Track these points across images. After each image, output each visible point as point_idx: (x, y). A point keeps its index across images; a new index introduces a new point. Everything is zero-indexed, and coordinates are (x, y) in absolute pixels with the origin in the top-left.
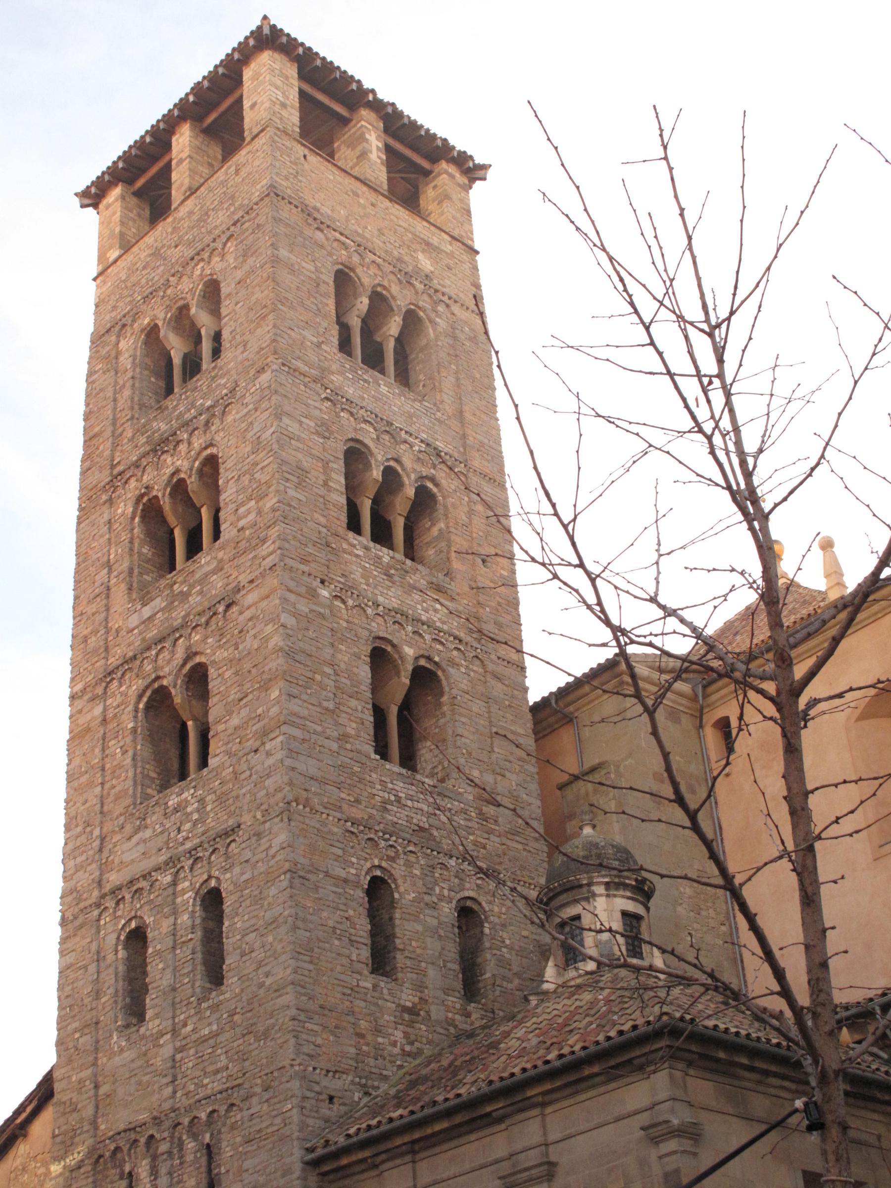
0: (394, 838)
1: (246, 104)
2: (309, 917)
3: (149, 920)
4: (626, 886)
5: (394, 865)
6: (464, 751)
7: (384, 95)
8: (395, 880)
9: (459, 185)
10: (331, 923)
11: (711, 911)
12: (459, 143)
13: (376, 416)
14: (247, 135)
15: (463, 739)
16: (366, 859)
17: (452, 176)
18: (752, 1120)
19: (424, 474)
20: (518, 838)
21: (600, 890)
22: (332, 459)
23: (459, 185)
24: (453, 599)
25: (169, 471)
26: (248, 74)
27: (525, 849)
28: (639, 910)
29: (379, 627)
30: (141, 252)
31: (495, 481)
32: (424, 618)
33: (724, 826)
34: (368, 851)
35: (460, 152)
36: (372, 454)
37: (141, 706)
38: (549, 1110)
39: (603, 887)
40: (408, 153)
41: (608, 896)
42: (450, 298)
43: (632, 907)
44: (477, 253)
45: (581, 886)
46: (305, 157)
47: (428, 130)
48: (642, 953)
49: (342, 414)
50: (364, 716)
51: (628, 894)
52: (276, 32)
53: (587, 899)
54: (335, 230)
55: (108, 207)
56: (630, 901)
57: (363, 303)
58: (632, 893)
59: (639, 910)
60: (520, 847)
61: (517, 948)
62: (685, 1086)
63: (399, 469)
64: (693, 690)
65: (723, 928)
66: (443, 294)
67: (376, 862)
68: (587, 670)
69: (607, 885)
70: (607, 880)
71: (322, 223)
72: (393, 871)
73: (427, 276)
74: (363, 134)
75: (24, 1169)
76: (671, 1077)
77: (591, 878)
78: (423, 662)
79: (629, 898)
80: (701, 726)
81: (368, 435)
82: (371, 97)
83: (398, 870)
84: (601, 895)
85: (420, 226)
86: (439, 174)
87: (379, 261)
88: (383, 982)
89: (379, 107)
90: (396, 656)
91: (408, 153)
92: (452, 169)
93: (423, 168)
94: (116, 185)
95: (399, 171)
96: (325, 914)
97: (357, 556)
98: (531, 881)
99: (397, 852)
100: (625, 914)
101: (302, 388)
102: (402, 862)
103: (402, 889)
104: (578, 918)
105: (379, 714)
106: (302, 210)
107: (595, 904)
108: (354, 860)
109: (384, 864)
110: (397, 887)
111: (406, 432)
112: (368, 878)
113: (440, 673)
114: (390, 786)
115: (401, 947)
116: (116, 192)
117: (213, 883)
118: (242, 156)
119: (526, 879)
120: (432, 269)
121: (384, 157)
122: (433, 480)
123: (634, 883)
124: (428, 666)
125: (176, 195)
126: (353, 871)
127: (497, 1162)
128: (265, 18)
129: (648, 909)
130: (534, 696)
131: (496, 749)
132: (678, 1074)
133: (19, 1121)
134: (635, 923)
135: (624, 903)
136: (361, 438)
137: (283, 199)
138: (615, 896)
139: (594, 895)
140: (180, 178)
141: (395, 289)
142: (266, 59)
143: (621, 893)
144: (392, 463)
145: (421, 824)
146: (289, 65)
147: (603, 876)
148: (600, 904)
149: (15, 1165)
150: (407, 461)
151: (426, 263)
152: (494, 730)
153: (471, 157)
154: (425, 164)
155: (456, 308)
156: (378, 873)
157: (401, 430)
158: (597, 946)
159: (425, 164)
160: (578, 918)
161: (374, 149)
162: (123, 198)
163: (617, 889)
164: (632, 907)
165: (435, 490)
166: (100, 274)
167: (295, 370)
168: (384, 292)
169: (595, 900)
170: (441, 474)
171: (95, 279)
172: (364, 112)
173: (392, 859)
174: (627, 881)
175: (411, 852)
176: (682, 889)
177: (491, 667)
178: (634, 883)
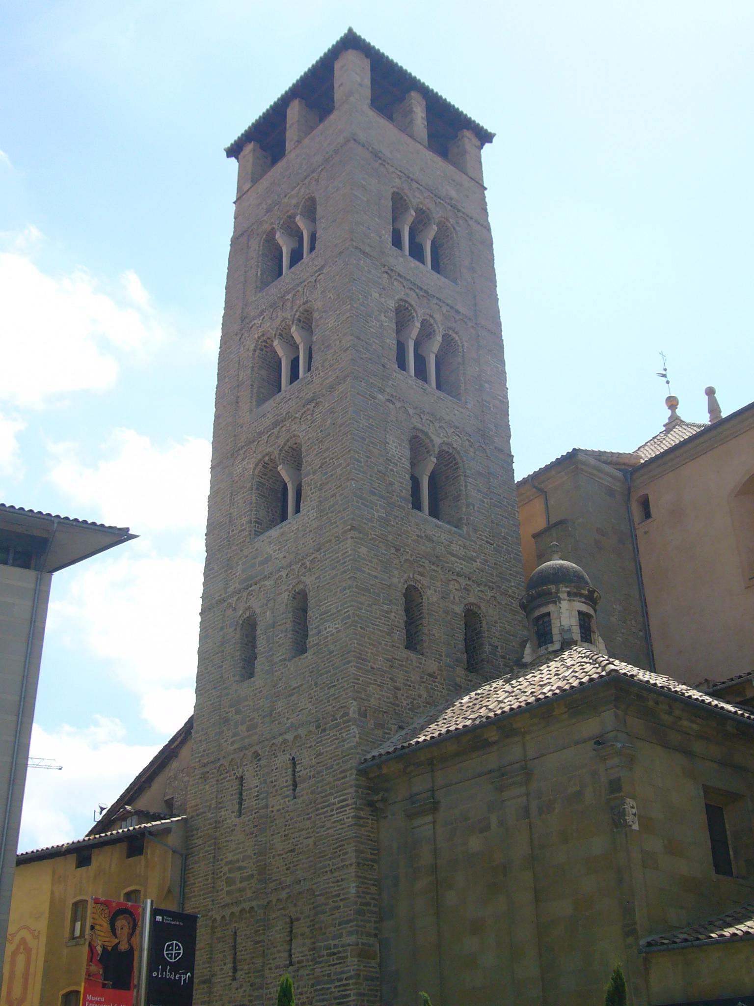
1: (336, 86)
3: (258, 610)
4: (581, 595)
9: (475, 146)
11: (633, 622)
14: (336, 105)
17: (470, 139)
18: (670, 748)
21: (563, 596)
23: (475, 146)
25: (278, 321)
26: (337, 66)
28: (591, 611)
29: (416, 422)
30: (264, 183)
33: (643, 566)
37: (256, 472)
38: (528, 737)
39: (566, 594)
41: (570, 600)
42: (467, 216)
43: (585, 608)
44: (486, 189)
45: (551, 593)
48: (591, 640)
49: (395, 283)
51: (583, 600)
53: (555, 602)
55: (244, 156)
57: (411, 215)
58: (586, 599)
59: (591, 611)
62: (625, 722)
63: (432, 321)
64: (624, 476)
65: (641, 634)
66: (464, 213)
68: (554, 460)
69: (569, 594)
70: (568, 589)
71: (384, 161)
74: (412, 108)
75: (175, 778)
76: (616, 715)
78: (445, 448)
79: (583, 602)
80: (629, 499)
81: (413, 300)
84: (565, 600)
85: (450, 168)
86: (463, 137)
87: (421, 187)
88: (413, 656)
94: (250, 142)
104: (548, 614)
105: (415, 483)
107: (560, 605)
115: (426, 632)
116: (250, 147)
117: (301, 586)
118: (333, 117)
121: (426, 123)
123: (587, 592)
125: (289, 146)
127: (490, 772)
129: (595, 611)
130: (518, 478)
132: (620, 713)
133: (173, 747)
134: (587, 619)
135: (580, 606)
138: (574, 601)
139: (560, 599)
140: (291, 134)
141: (432, 206)
142: (351, 57)
143: (578, 598)
144: (428, 318)
148: (564, 605)
149: (170, 775)
150: (438, 317)
151: (453, 194)
155: (471, 222)
156: (412, 583)
158: (561, 634)
160: (548, 614)
162: (254, 150)
164: (585, 608)
166: (238, 199)
169: (560, 603)
171: (235, 203)
172: (414, 94)
176: (615, 607)
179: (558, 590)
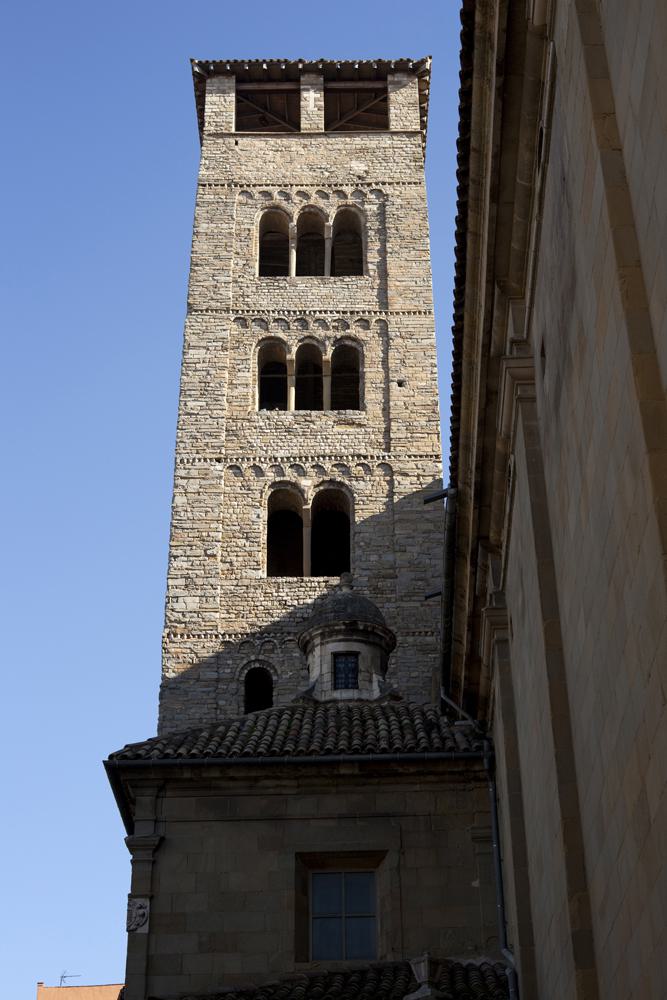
0: (272, 635)
2: (176, 716)
4: (338, 632)
5: (272, 655)
6: (362, 544)
7: (311, 58)
8: (273, 667)
10: (197, 716)
12: (392, 57)
13: (289, 312)
15: (362, 535)
16: (243, 658)
18: (239, 820)
19: (338, 337)
20: (415, 598)
21: (317, 641)
22: (239, 362)
24: (360, 425)
27: (422, 606)
31: (420, 313)
32: (328, 451)
34: (244, 651)
35: (396, 63)
36: (285, 343)
40: (360, 85)
43: (341, 647)
46: (237, 143)
47: (360, 63)
50: (252, 549)
51: (341, 637)
52: (203, 65)
54: (260, 185)
56: (342, 643)
58: (344, 635)
60: (418, 604)
61: (403, 688)
63: (315, 343)
66: (377, 184)
67: (253, 658)
69: (322, 635)
72: (271, 661)
73: (359, 177)
77: (310, 634)
79: (340, 641)
82: (300, 66)
83: (275, 658)
89: (310, 69)
90: (295, 491)
91: (360, 85)
92: (398, 77)
93: (378, 89)
95: (376, 98)
96: (193, 711)
97: (261, 428)
98: (427, 630)
99: (275, 644)
100: (336, 655)
101: (212, 320)
102: (279, 651)
103: (279, 672)
106: (229, 185)
108: (230, 662)
109: (261, 657)
110: (276, 671)
111: (320, 312)
112: (246, 671)
113: (344, 490)
114: (276, 594)
119: (422, 629)
120: (367, 168)
122: (349, 338)
123: (343, 627)
124: (331, 487)
126: (229, 671)
128: (192, 61)
131: (396, 532)
136: (273, 335)
137: (210, 185)
138: (328, 642)
141: (321, 203)
144: (307, 341)
145: (306, 616)
146: (226, 80)
147: (317, 629)
148: (317, 651)
151: (359, 167)
152: (396, 517)
153: (409, 60)
154: (378, 85)
155: (387, 189)
157: (315, 312)
159: (378, 85)
161: (312, 103)
163: (331, 636)
165: (354, 344)
167: (207, 310)
168: (312, 210)
170: (354, 330)
173: (272, 651)
174: (336, 628)
175: (290, 640)
177: (396, 466)
178: (343, 627)
179: (312, 638)
